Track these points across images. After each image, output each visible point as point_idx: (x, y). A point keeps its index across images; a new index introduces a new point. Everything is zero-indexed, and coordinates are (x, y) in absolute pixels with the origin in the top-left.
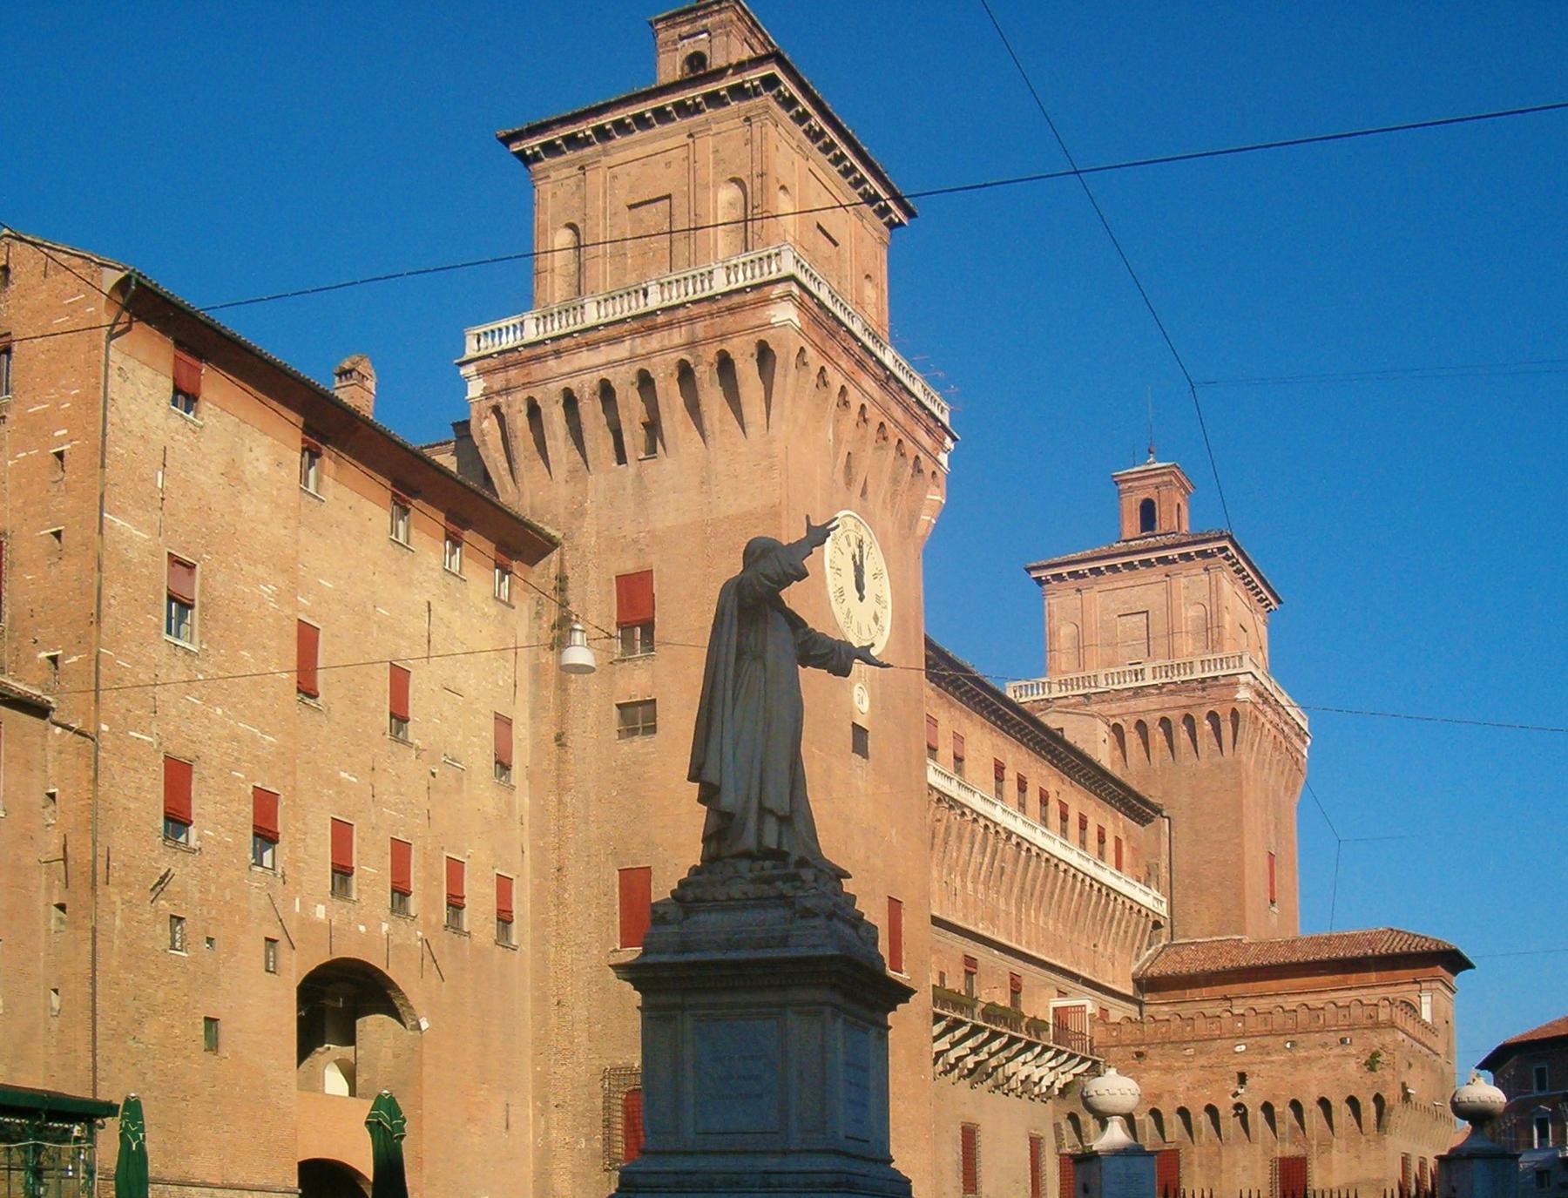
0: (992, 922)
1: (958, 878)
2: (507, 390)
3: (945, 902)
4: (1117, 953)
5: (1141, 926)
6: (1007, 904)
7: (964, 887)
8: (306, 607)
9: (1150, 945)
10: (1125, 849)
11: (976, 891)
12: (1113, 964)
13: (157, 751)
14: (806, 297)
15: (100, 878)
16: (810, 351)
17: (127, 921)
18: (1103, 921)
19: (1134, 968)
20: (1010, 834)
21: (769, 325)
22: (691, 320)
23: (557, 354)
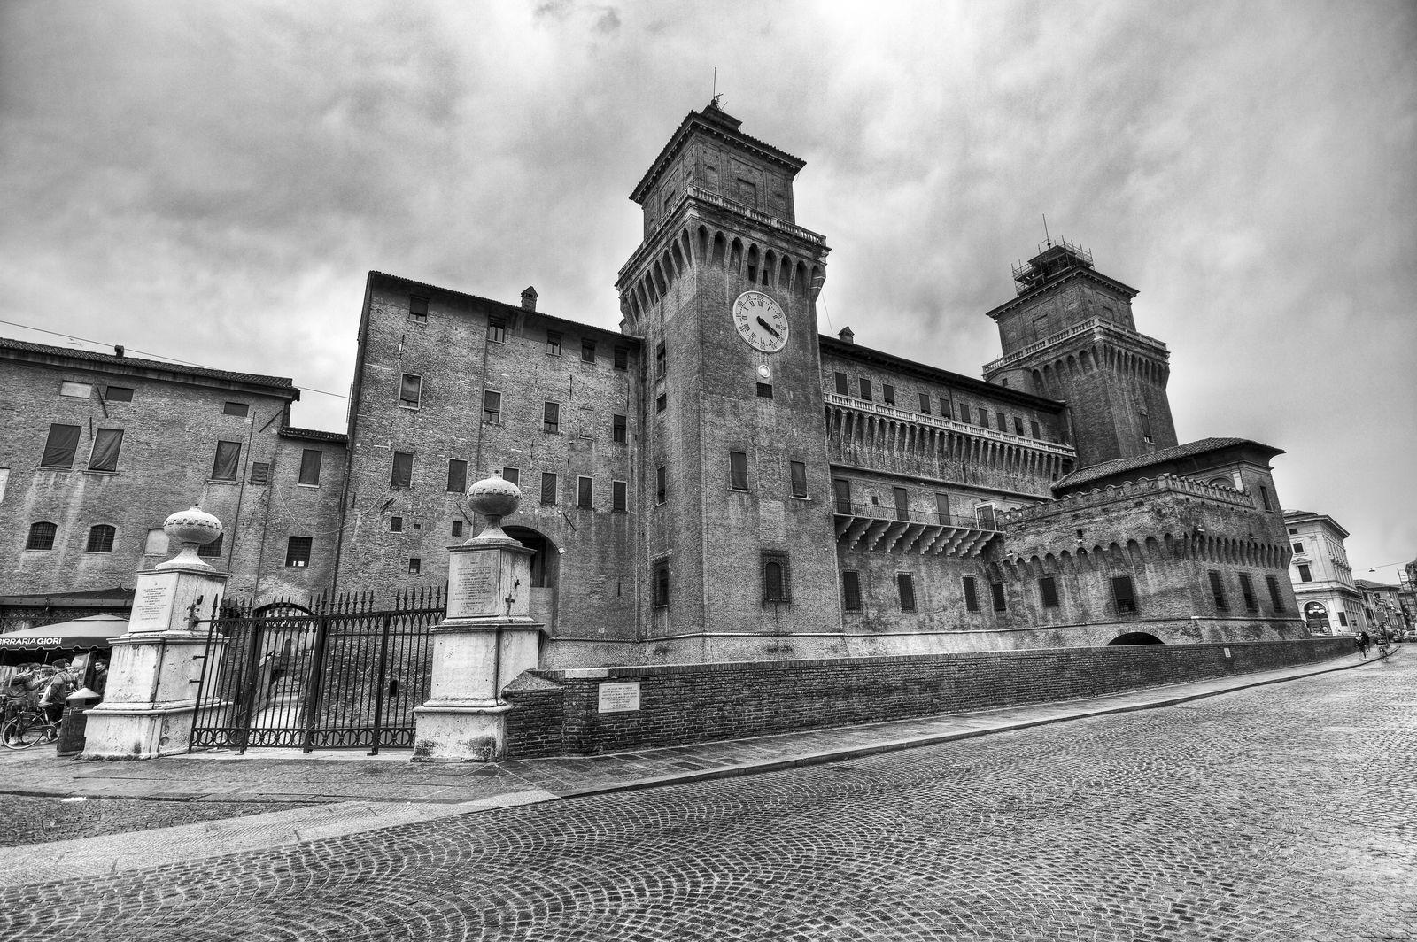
0: (918, 469)
2: (627, 289)
4: (1036, 478)
7: (891, 454)
8: (492, 385)
9: (1065, 472)
10: (1041, 427)
11: (902, 456)
12: (1033, 484)
13: (391, 451)
14: (702, 205)
15: (349, 506)
16: (708, 226)
17: (364, 522)
19: (1053, 484)
20: (923, 427)
21: (686, 221)
22: (666, 233)
23: (637, 268)
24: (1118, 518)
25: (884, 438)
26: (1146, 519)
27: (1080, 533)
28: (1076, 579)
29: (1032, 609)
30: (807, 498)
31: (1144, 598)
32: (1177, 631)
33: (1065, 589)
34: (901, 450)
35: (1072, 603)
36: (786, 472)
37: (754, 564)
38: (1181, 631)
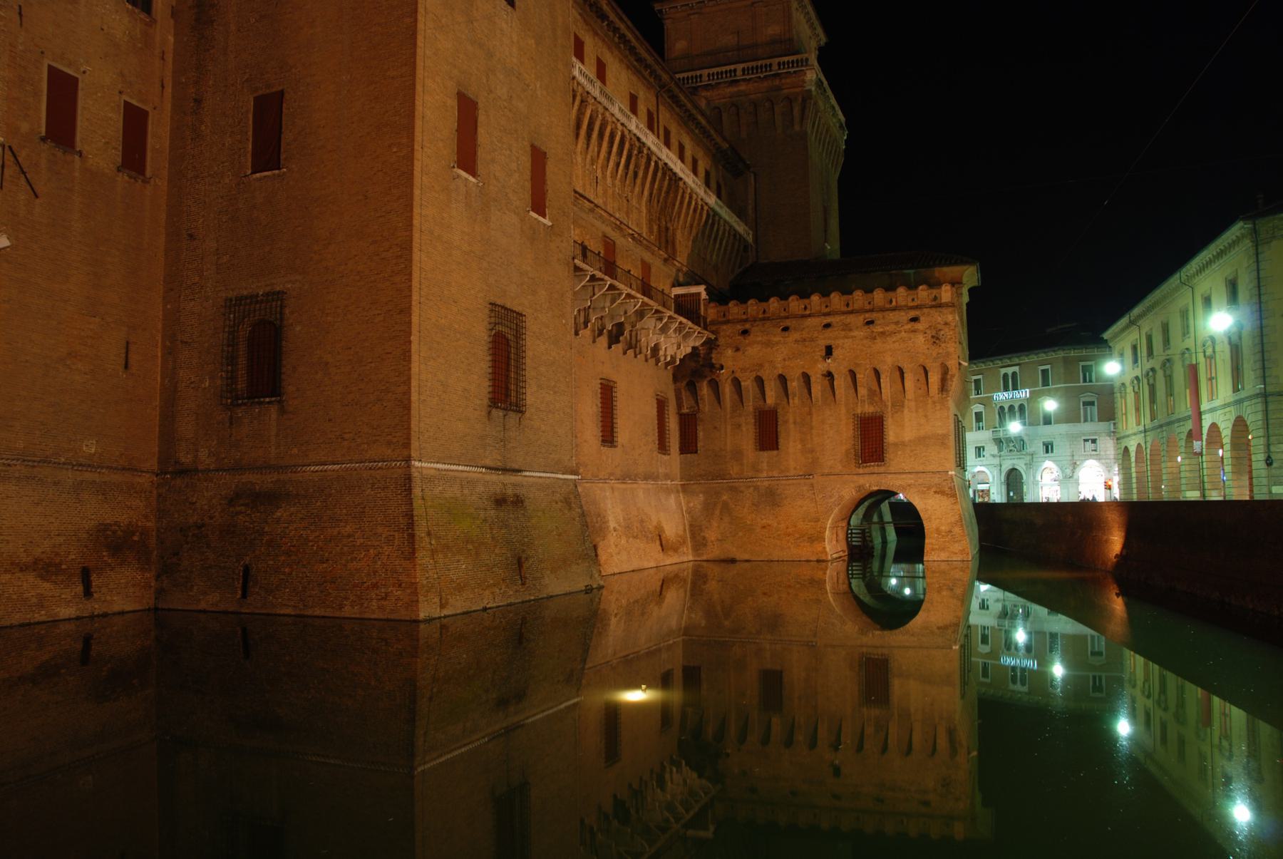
0: (627, 214)
1: (599, 171)
3: (588, 186)
5: (736, 247)
6: (639, 202)
7: (604, 177)
18: (710, 236)
24: (883, 333)
25: (600, 146)
26: (920, 340)
27: (829, 351)
28: (810, 413)
29: (738, 455)
30: (547, 222)
31: (896, 445)
32: (929, 488)
33: (792, 426)
34: (614, 176)
35: (799, 446)
36: (526, 161)
37: (481, 333)
38: (933, 489)
